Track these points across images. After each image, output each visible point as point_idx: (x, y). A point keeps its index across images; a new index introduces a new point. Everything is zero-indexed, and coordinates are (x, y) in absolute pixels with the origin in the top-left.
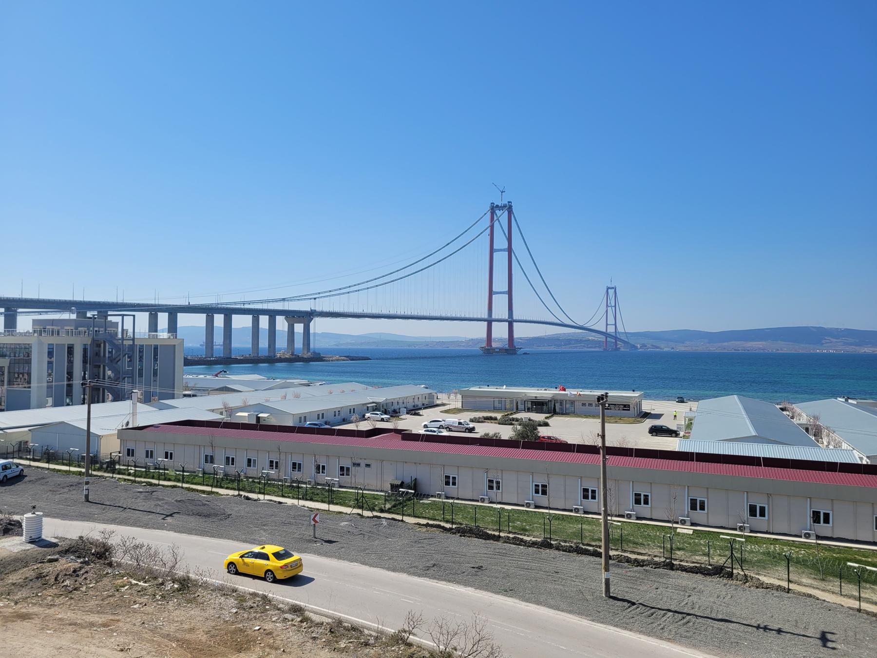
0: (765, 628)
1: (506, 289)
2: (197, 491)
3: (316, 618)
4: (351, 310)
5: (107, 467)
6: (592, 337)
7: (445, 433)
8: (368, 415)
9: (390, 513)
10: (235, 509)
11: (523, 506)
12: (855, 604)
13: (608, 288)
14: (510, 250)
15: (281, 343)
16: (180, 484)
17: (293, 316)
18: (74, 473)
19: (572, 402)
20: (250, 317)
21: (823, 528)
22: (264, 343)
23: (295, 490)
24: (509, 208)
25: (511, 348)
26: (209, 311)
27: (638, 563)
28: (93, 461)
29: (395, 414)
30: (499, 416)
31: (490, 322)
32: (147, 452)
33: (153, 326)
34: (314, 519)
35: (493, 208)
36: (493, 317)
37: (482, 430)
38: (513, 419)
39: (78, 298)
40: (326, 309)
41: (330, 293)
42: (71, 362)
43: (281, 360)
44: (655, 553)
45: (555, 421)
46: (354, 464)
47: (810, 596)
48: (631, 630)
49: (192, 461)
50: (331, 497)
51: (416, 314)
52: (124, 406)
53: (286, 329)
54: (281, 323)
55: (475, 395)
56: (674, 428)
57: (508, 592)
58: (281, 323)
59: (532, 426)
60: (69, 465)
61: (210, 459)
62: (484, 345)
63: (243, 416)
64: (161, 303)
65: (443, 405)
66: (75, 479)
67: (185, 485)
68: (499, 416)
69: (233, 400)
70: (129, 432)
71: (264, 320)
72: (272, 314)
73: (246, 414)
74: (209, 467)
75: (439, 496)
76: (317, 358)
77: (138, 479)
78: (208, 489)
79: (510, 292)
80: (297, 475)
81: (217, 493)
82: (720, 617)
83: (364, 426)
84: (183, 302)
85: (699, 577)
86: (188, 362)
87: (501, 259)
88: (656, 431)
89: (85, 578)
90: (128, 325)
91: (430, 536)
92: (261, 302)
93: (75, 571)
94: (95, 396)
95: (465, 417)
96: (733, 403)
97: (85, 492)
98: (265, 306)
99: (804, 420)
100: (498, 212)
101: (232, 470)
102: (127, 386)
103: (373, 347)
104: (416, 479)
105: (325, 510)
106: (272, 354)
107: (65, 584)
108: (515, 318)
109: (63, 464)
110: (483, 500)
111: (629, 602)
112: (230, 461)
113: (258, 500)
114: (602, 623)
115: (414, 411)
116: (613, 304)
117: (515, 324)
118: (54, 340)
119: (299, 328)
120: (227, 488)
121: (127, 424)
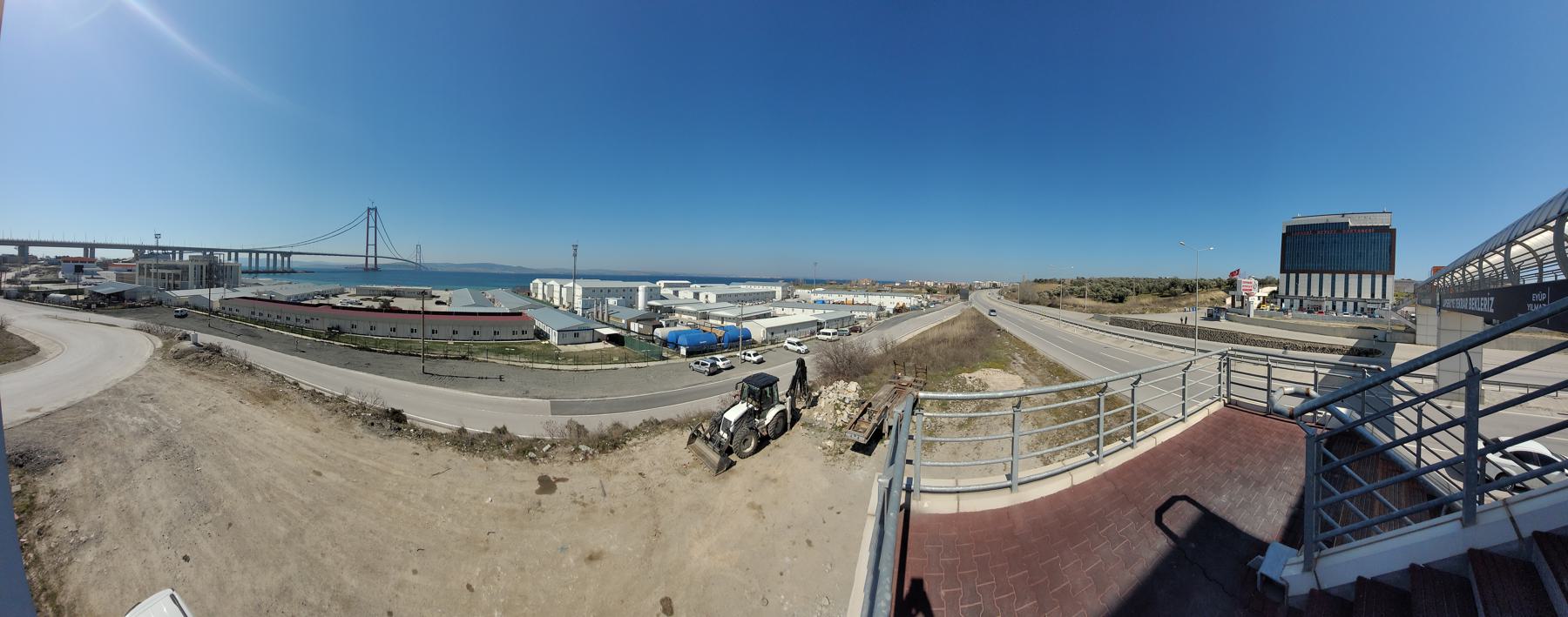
3: (305, 388)
6: (410, 264)
7: (350, 305)
17: (284, 254)
20: (248, 254)
22: (271, 264)
25: (376, 268)
26: (250, 252)
31: (367, 257)
33: (229, 259)
35: (369, 209)
37: (366, 304)
39: (203, 247)
41: (305, 243)
42: (202, 272)
43: (278, 272)
45: (396, 299)
52: (221, 289)
55: (361, 289)
59: (387, 302)
61: (253, 313)
68: (372, 298)
70: (223, 300)
71: (272, 256)
86: (243, 273)
87: (372, 231)
90: (222, 258)
94: (210, 286)
96: (466, 291)
101: (261, 318)
102: (221, 283)
115: (335, 296)
118: (196, 263)
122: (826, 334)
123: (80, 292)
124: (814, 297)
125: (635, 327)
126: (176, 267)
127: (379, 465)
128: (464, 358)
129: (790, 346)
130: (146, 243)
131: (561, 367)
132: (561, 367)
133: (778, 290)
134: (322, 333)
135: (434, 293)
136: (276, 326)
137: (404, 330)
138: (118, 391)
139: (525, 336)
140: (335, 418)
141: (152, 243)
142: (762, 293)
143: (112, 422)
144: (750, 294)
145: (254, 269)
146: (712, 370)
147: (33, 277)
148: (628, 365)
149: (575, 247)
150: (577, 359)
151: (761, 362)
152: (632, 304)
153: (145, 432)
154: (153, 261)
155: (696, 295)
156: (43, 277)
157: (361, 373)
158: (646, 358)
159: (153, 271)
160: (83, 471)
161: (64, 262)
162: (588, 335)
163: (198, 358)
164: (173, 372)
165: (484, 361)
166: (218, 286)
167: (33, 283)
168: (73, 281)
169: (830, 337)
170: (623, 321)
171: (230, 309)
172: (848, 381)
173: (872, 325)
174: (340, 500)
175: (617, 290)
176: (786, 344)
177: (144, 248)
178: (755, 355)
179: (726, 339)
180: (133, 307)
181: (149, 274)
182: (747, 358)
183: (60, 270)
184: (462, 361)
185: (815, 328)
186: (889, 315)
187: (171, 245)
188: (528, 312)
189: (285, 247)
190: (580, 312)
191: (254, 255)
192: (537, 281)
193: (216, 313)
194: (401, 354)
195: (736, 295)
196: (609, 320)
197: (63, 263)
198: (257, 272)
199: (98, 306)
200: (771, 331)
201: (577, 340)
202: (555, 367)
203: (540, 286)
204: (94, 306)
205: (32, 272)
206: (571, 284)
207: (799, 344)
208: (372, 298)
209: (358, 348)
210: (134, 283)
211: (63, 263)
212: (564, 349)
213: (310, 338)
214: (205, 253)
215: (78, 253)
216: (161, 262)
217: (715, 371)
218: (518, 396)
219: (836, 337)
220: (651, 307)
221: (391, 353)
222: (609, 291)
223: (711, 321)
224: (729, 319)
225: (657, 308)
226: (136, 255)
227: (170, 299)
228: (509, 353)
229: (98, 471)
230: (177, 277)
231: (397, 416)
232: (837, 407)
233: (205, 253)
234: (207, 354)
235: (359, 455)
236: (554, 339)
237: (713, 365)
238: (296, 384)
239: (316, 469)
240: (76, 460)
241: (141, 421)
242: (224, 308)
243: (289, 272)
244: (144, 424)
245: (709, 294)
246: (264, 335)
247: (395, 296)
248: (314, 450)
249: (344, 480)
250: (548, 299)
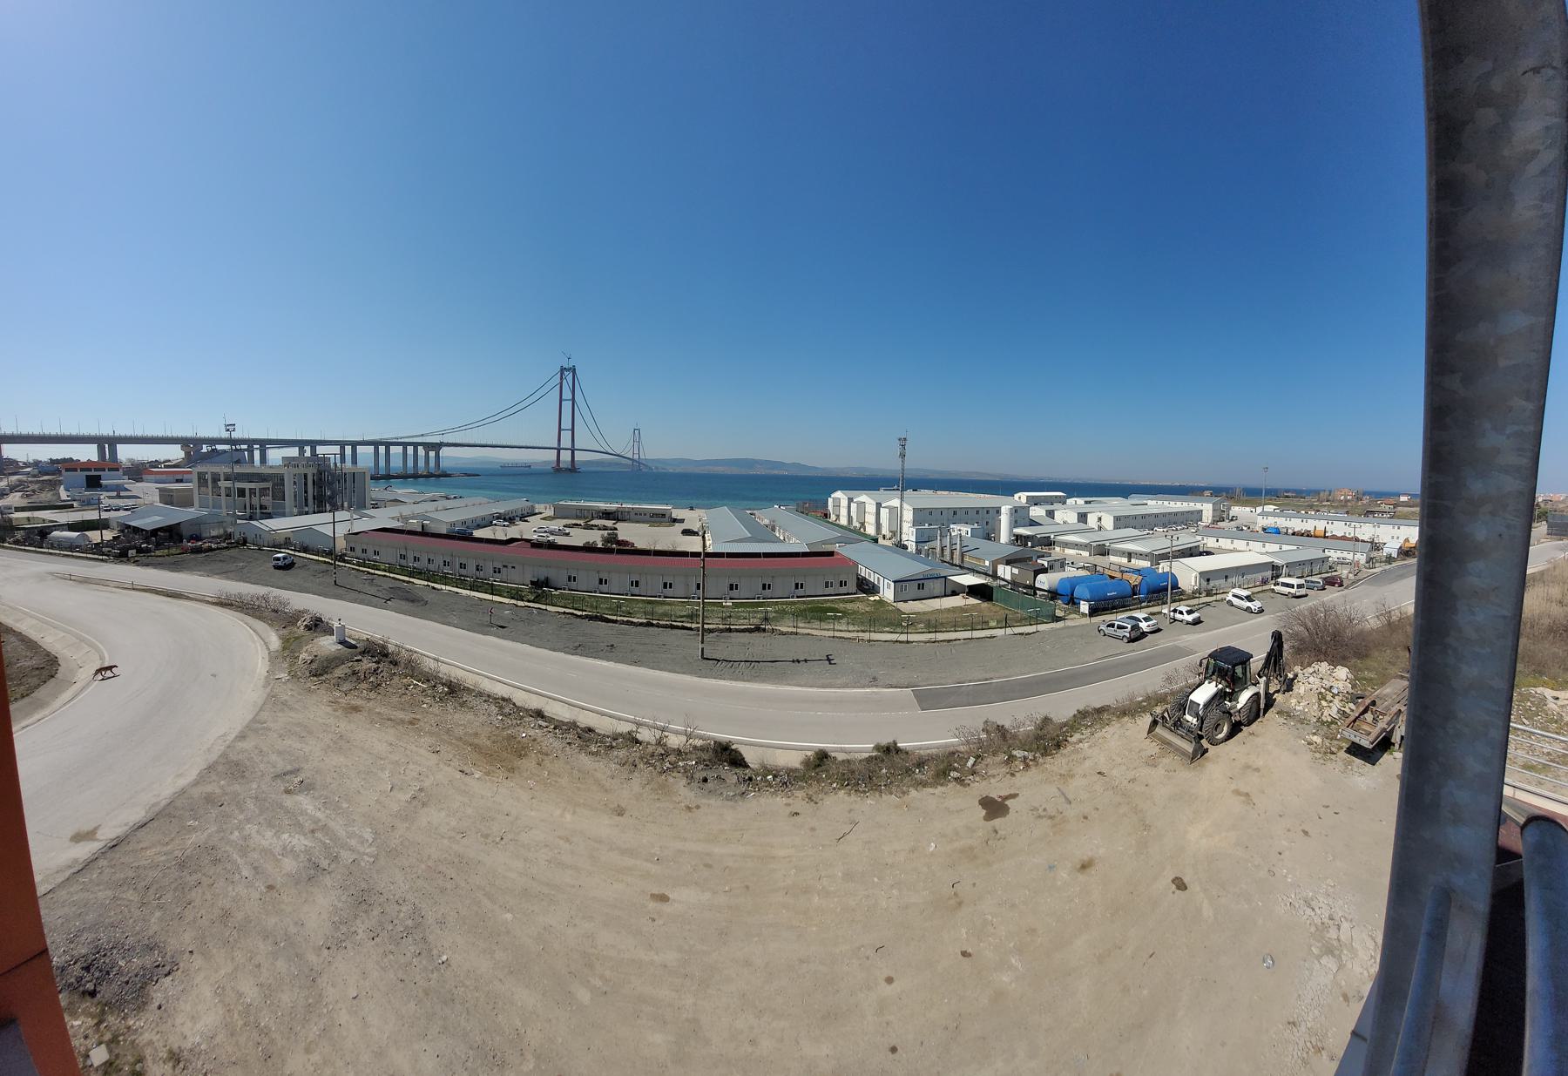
4: (464, 442)
6: (624, 461)
17: (429, 446)
22: (410, 463)
25: (573, 469)
26: (376, 444)
43: (422, 476)
71: (410, 449)
72: (416, 445)
84: (359, 439)
87: (567, 406)
103: (479, 466)
108: (576, 447)
122: (1287, 585)
124: (1262, 522)
125: (1005, 572)
128: (758, 629)
129: (1236, 601)
131: (912, 637)
132: (912, 637)
133: (1207, 509)
134: (521, 590)
135: (677, 514)
136: (445, 580)
137: (652, 585)
138: (231, 767)
139: (844, 590)
142: (1182, 513)
143: (244, 852)
144: (1164, 515)
145: (382, 472)
146: (1134, 634)
147: (15, 499)
148: (1009, 631)
149: (903, 442)
150: (933, 624)
151: (1197, 622)
152: (990, 535)
153: (313, 872)
155: (1083, 517)
156: (34, 498)
157: (605, 663)
158: (1035, 619)
160: (219, 991)
161: (67, 470)
162: (937, 587)
163: (354, 673)
164: (318, 708)
165: (792, 633)
167: (18, 509)
168: (87, 504)
169: (1293, 591)
170: (987, 563)
171: (364, 551)
172: (1334, 663)
173: (1360, 576)
175: (967, 511)
176: (1230, 597)
177: (199, 442)
178: (1189, 612)
179: (1144, 589)
180: (198, 551)
182: (1178, 616)
183: (60, 483)
185: (1269, 574)
186: (1389, 559)
187: (246, 436)
189: (432, 434)
190: (912, 547)
191: (382, 449)
192: (838, 494)
193: (342, 558)
194: (658, 626)
195: (1144, 516)
196: (962, 561)
198: (388, 477)
200: (1207, 576)
201: (921, 593)
202: (903, 637)
204: (132, 553)
205: (13, 489)
206: (896, 503)
207: (1249, 599)
208: (581, 522)
209: (587, 616)
210: (192, 505)
211: (63, 471)
212: (901, 606)
213: (506, 600)
214: (302, 451)
215: (89, 453)
217: (1138, 636)
219: (1302, 591)
220: (1018, 537)
221: (641, 624)
222: (955, 513)
223: (1113, 559)
224: (1141, 556)
225: (1027, 538)
226: (188, 454)
227: (259, 534)
229: (251, 993)
232: (1322, 697)
233: (302, 451)
234: (367, 664)
236: (888, 593)
237: (1135, 628)
240: (198, 961)
241: (300, 842)
244: (307, 851)
245: (1103, 514)
246: (429, 597)
247: (618, 520)
250: (856, 524)
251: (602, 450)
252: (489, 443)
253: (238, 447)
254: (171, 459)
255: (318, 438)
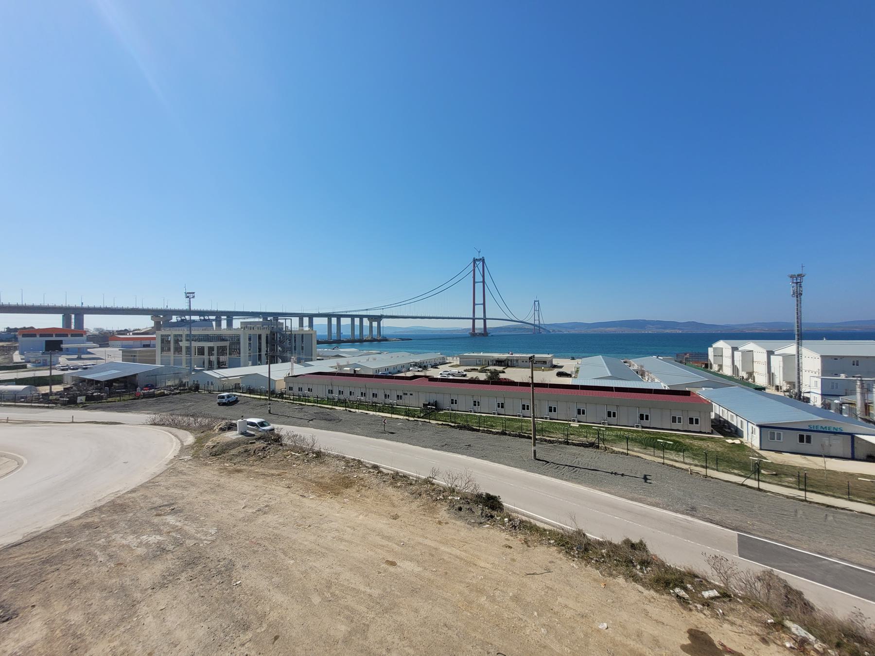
0: (616, 474)
1: (482, 302)
2: (325, 408)
5: (279, 396)
7: (451, 377)
8: (411, 368)
9: (423, 418)
10: (343, 417)
11: (491, 414)
12: (661, 461)
13: (535, 301)
14: (484, 282)
15: (366, 332)
16: (316, 405)
17: (372, 318)
18: (263, 399)
19: (517, 361)
21: (645, 423)
22: (357, 332)
23: (374, 407)
24: (483, 260)
25: (485, 333)
26: (329, 316)
27: (551, 442)
28: (272, 393)
29: (425, 368)
30: (479, 368)
31: (474, 319)
32: (299, 388)
33: (301, 324)
34: (384, 422)
35: (475, 261)
36: (476, 317)
37: (470, 375)
38: (486, 370)
40: (389, 314)
41: (390, 306)
42: (260, 343)
43: (366, 341)
44: (560, 437)
45: (508, 370)
46: (404, 394)
47: (638, 457)
48: (547, 476)
49: (320, 391)
50: (392, 410)
51: (435, 316)
52: (288, 365)
53: (368, 325)
54: (366, 322)
55: (467, 357)
56: (569, 372)
57: (483, 457)
58: (365, 321)
59: (496, 373)
60: (261, 395)
61: (331, 392)
62: (471, 331)
63: (347, 370)
64: (305, 312)
65: (450, 363)
66: (263, 402)
67: (318, 405)
68: (479, 368)
69: (342, 362)
71: (357, 321)
72: (361, 317)
73: (349, 369)
74: (330, 396)
75: (448, 410)
76: (385, 339)
77: (295, 402)
78: (330, 407)
79: (484, 304)
80: (375, 400)
81: (335, 409)
82: (592, 468)
83: (409, 374)
84: (316, 312)
85: (582, 448)
86: (319, 343)
87: (479, 287)
88: (560, 374)
89: (269, 452)
90: (288, 324)
91: (444, 430)
92: (355, 311)
93: (263, 448)
94: (272, 360)
95: (461, 369)
96: (599, 359)
97: (269, 409)
98: (357, 313)
99: (636, 367)
100: (477, 263)
101: (342, 397)
102: (288, 355)
104: (436, 401)
105: (389, 417)
106: (361, 338)
107: (259, 454)
109: (258, 395)
110: (471, 411)
111: (546, 461)
112: (340, 392)
113: (356, 412)
114: (532, 472)
115: (435, 366)
116: (538, 309)
117: (487, 320)
118: (252, 332)
119: (375, 324)
120: (340, 406)
121: (289, 374)
123: (57, 380)
126: (220, 338)
127: (463, 555)
130: (173, 306)
140: (417, 503)
141: (184, 306)
154: (184, 331)
159: (184, 344)
166: (284, 360)
174: (414, 591)
181: (178, 349)
183: (15, 349)
184: (590, 449)
187: (214, 309)
188: (703, 393)
190: (816, 400)
197: (20, 338)
199: (90, 398)
203: (727, 352)
211: (20, 338)
216: (196, 332)
218: (676, 511)
228: (664, 448)
230: (222, 351)
231: (492, 503)
235: (441, 542)
238: (375, 467)
239: (390, 560)
242: (291, 389)
243: (379, 341)
248: (389, 538)
249: (420, 569)
251: (509, 319)
252: (419, 315)
253: (206, 318)
254: (141, 328)
255: (280, 311)
